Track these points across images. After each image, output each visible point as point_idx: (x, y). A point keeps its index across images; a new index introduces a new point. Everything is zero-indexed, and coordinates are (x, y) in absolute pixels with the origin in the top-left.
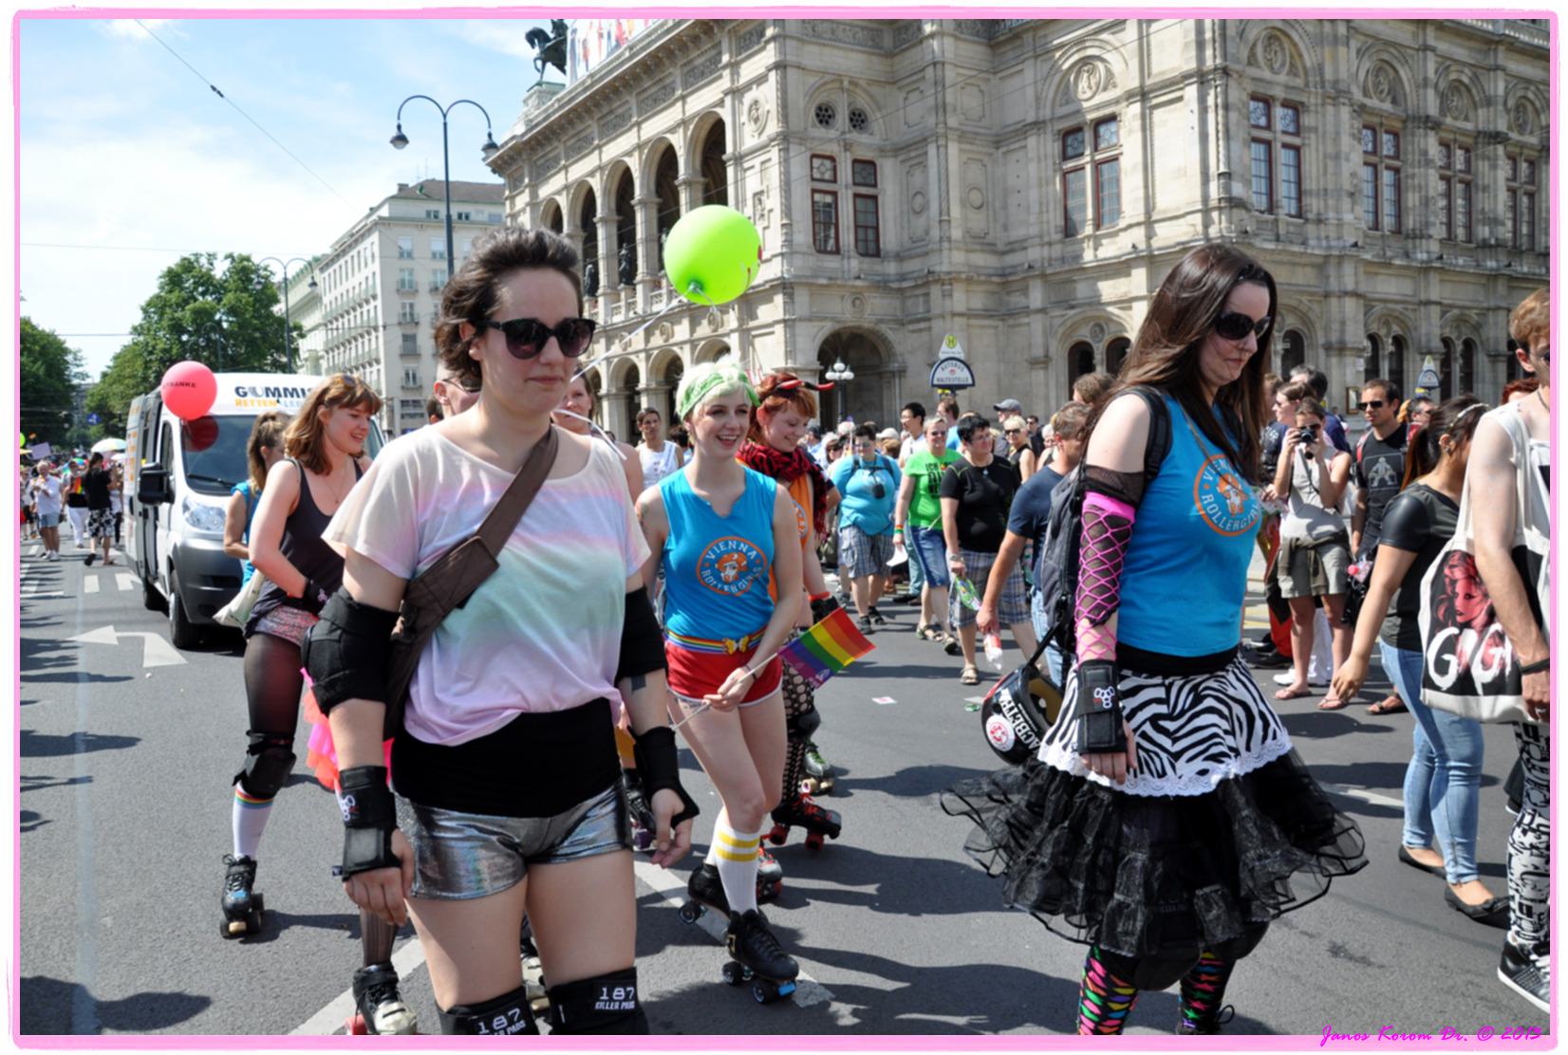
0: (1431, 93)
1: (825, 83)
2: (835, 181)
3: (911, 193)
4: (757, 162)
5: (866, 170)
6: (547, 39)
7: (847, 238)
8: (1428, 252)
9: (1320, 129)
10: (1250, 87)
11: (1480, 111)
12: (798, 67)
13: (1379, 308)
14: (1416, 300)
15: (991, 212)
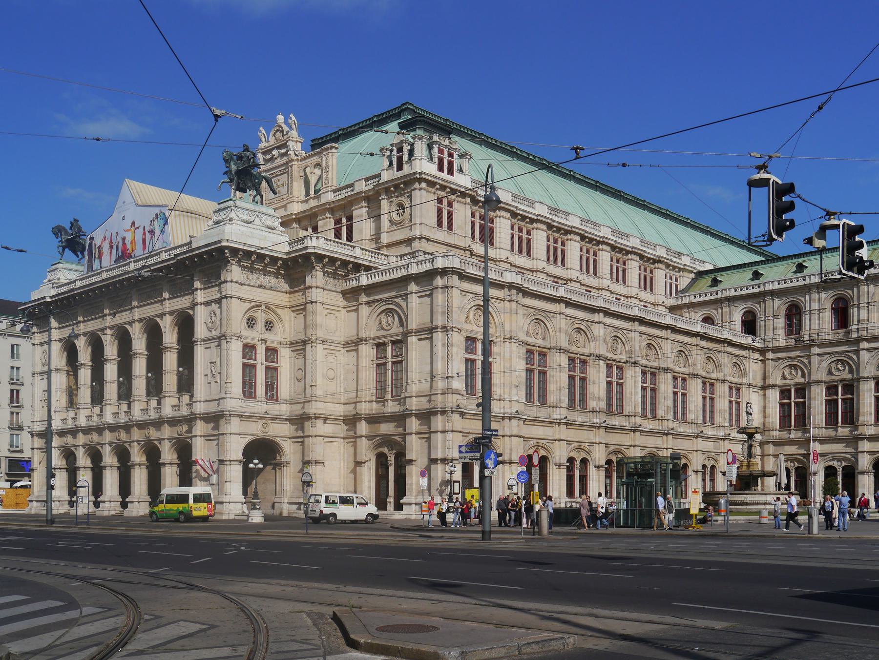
0: (563, 335)
1: (252, 307)
2: (255, 359)
3: (297, 368)
4: (213, 345)
5: (271, 352)
6: (66, 233)
7: (261, 390)
8: (560, 415)
9: (502, 353)
10: (465, 335)
11: (591, 343)
12: (239, 299)
13: (532, 442)
14: (554, 438)
15: (339, 381)
